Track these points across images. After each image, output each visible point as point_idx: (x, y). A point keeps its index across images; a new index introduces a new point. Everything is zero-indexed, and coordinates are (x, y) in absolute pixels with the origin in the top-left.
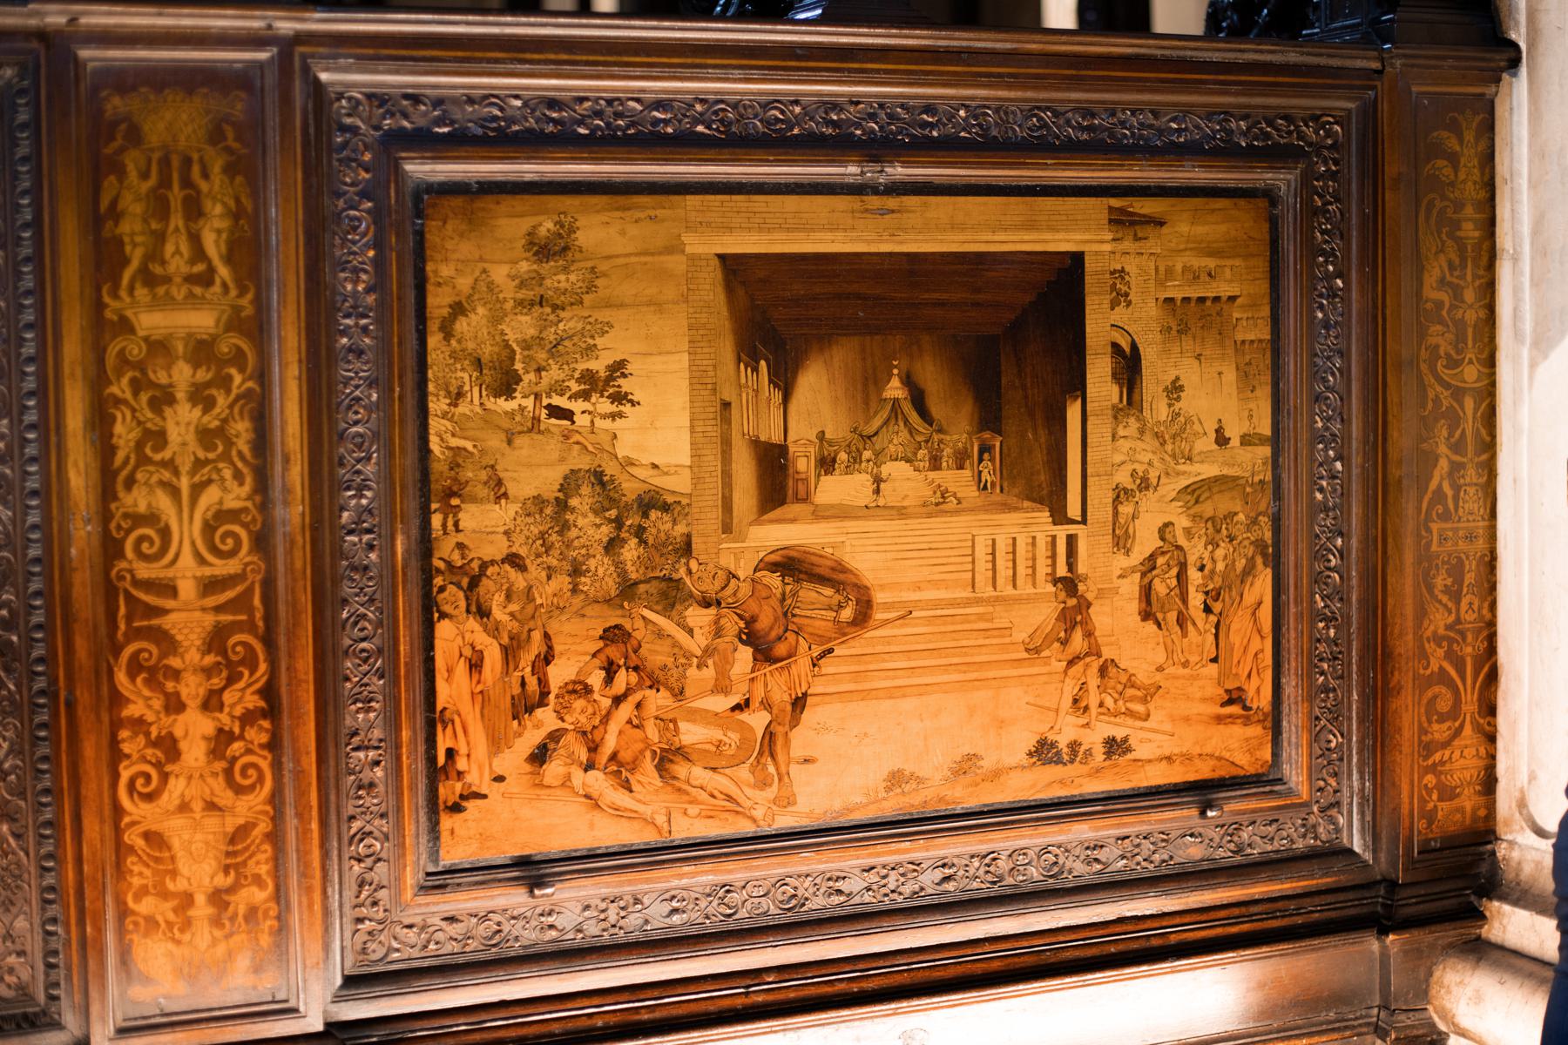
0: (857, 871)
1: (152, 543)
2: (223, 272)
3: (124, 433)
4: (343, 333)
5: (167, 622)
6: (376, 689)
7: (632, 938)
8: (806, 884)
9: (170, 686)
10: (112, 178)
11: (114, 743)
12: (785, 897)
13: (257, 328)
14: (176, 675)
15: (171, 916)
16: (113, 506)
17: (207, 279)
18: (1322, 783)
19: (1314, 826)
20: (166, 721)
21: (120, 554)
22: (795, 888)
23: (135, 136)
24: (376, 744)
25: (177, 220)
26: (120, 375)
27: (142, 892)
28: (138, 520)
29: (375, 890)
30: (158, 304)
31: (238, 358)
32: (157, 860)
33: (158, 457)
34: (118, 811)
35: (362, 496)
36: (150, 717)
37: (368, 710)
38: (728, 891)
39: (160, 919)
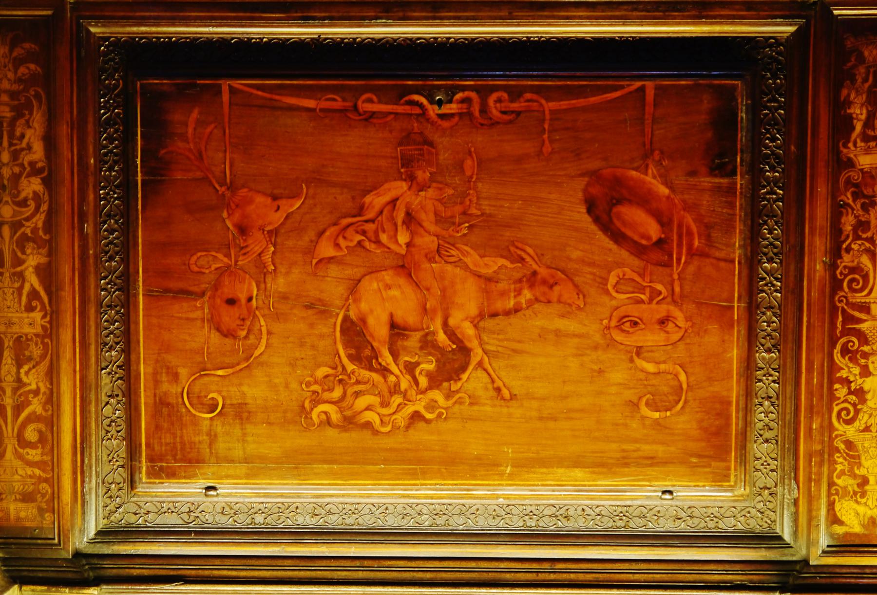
1: (858, 284)
3: (848, 223)
5: (863, 327)
9: (863, 361)
10: (848, 82)
11: (831, 390)
14: (866, 355)
15: (856, 489)
16: (839, 261)
20: (860, 381)
21: (842, 289)
23: (861, 59)
26: (847, 190)
27: (843, 473)
28: (853, 270)
30: (868, 151)
32: (853, 457)
33: (864, 236)
34: (831, 427)
36: (851, 378)
39: (850, 489)
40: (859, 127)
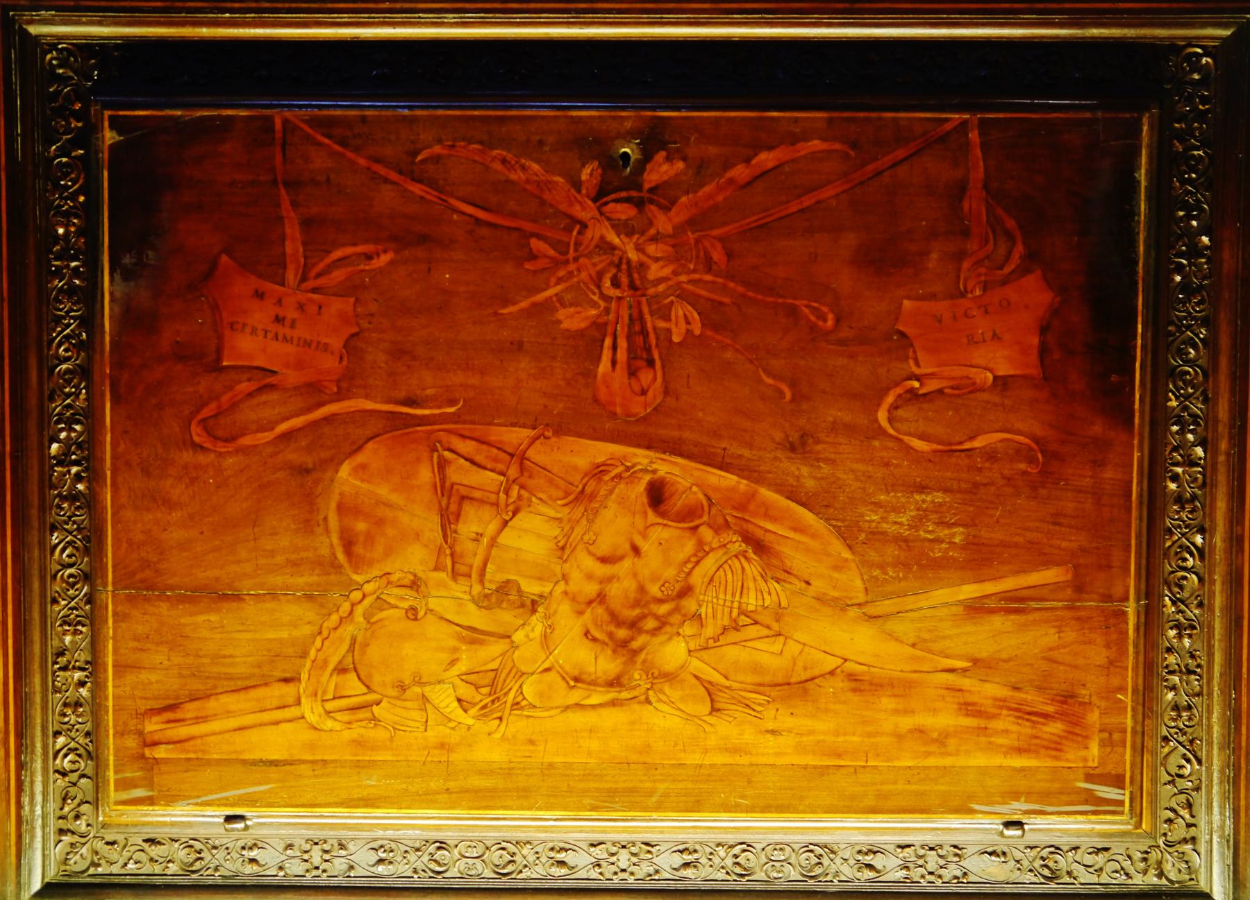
0: (585, 846)
4: (58, 274)
6: (83, 613)
7: (334, 882)
8: (525, 852)
12: (502, 862)
18: (1171, 815)
19: (1159, 863)
22: (513, 855)
24: (83, 666)
29: (79, 805)
35: (72, 430)
37: (76, 632)
38: (439, 848)
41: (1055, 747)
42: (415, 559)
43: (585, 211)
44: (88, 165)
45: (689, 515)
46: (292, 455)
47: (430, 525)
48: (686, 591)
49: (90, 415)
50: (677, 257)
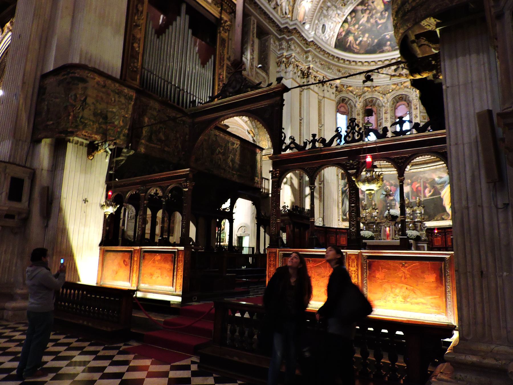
2: (356, 266)
13: (358, 270)
17: (355, 267)
23: (351, 258)
25: (353, 263)
31: (356, 272)
40: (351, 265)
41: (439, 310)
42: (389, 292)
43: (401, 268)
44: (367, 263)
45: (409, 290)
46: (381, 284)
47: (391, 290)
48: (409, 296)
49: (367, 280)
50: (408, 271)
